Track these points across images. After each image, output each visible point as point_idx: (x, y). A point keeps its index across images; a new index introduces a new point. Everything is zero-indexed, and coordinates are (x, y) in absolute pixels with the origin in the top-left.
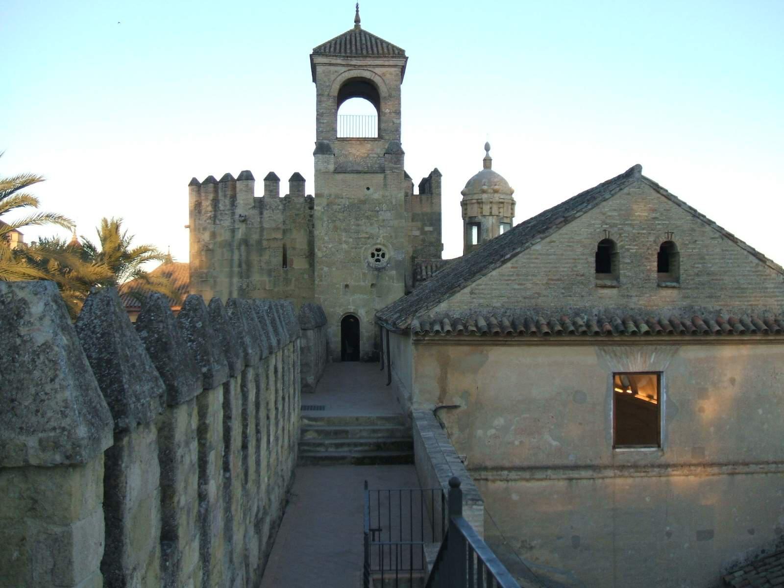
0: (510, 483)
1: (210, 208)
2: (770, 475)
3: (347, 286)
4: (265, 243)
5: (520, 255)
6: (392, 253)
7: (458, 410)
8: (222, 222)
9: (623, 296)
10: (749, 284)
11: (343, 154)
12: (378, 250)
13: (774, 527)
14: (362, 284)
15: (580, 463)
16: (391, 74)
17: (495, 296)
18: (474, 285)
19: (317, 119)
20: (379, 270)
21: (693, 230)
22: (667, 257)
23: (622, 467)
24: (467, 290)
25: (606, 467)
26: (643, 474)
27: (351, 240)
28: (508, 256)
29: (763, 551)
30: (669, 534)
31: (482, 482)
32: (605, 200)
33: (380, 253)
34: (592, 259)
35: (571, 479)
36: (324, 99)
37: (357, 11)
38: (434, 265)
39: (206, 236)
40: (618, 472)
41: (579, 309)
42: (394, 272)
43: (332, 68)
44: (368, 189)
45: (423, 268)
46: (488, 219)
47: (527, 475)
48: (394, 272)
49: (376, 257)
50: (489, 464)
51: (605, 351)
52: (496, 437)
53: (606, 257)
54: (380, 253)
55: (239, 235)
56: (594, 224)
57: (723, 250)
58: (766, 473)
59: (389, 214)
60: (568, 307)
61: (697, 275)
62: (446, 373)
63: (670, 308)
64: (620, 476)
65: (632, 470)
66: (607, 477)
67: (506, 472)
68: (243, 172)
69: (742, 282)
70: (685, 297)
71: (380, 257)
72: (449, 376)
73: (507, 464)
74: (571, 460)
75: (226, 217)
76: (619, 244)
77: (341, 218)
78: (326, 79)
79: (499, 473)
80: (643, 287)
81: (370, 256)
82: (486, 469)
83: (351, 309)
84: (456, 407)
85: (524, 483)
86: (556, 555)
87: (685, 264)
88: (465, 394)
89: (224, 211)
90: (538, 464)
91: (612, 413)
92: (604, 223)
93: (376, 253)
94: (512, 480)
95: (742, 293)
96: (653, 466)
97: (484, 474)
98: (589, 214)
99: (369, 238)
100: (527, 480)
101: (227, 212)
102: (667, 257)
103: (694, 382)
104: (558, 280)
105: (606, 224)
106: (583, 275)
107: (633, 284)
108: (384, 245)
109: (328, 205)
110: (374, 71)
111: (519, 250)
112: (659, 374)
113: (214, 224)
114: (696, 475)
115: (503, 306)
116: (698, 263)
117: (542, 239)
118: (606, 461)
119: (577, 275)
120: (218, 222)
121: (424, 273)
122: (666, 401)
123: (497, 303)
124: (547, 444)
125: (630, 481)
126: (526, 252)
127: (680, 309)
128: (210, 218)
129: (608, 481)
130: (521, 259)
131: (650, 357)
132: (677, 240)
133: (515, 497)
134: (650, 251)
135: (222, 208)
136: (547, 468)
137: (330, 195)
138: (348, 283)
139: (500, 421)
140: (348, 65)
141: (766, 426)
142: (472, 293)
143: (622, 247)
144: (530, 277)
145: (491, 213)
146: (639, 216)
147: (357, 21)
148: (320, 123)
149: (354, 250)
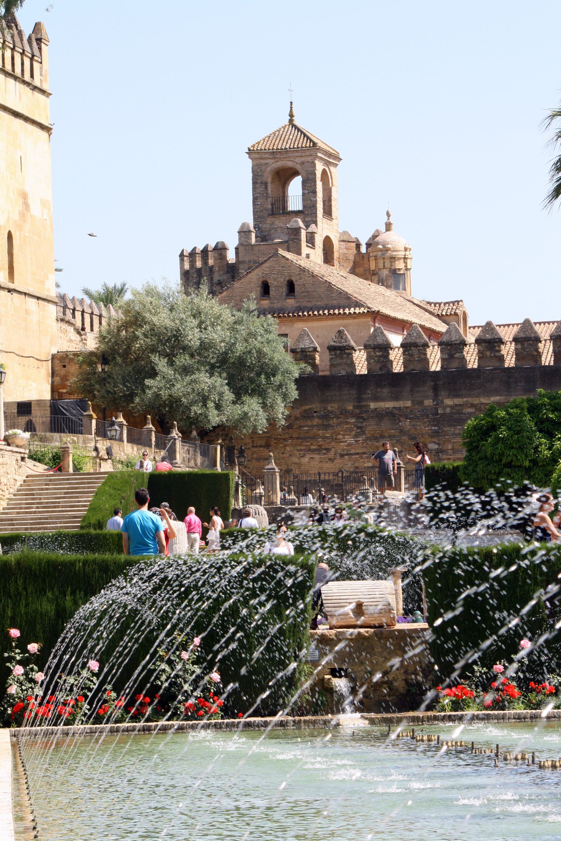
1: (195, 275)
16: (308, 162)
19: (254, 202)
22: (291, 287)
36: (257, 185)
37: (291, 108)
43: (263, 161)
68: (218, 243)
70: (298, 302)
78: (259, 170)
87: (297, 288)
102: (291, 287)
132: (294, 279)
137: (250, 261)
140: (274, 158)
145: (384, 266)
147: (291, 115)
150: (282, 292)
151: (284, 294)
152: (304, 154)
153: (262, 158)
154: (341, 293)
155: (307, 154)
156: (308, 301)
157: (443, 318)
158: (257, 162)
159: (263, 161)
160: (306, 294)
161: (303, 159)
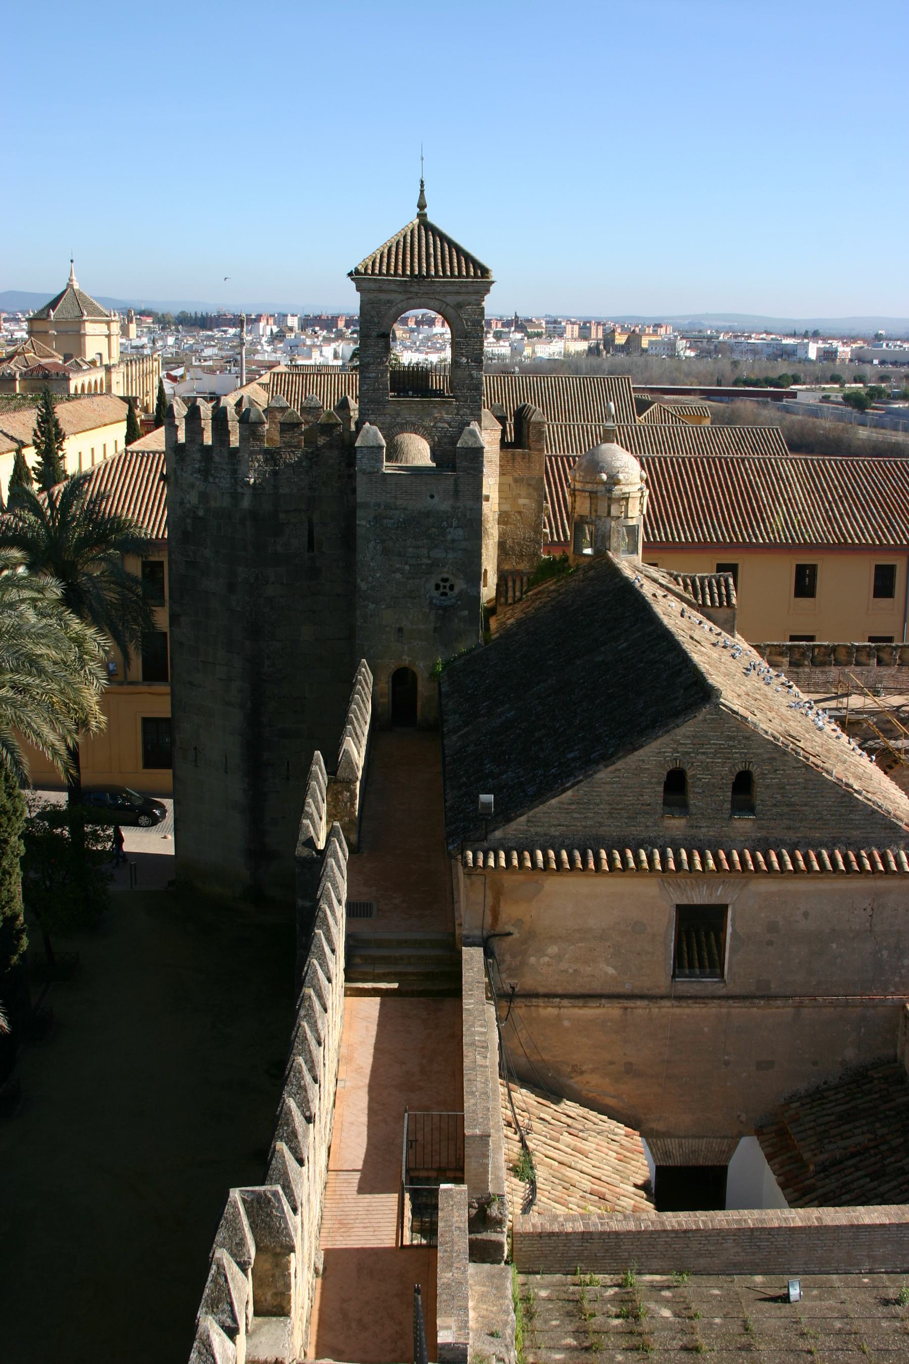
0: (562, 1010)
1: (198, 456)
2: (839, 1009)
3: (400, 630)
4: (282, 516)
5: (582, 784)
6: (464, 586)
7: (511, 938)
8: (217, 480)
9: (692, 827)
10: (832, 815)
11: (398, 423)
12: (445, 580)
13: (840, 1059)
14: (422, 627)
15: (636, 991)
17: (554, 826)
18: (531, 813)
20: (445, 609)
21: (774, 759)
22: (743, 783)
23: (679, 998)
24: (523, 819)
25: (662, 997)
26: (702, 1005)
27: (407, 567)
28: (569, 784)
29: (825, 1083)
30: (727, 1063)
31: (533, 1008)
32: (678, 726)
33: (448, 584)
34: (661, 789)
35: (626, 1008)
37: (422, 192)
38: (525, 579)
39: (193, 498)
40: (675, 1003)
41: (643, 840)
42: (466, 613)
43: (383, 296)
44: (432, 497)
45: (510, 584)
46: (605, 522)
47: (580, 1002)
48: (466, 613)
49: (442, 590)
50: (541, 990)
51: (669, 884)
52: (549, 965)
53: (676, 784)
54: (448, 584)
55: (246, 503)
56: (664, 752)
57: (806, 780)
58: (835, 1007)
59: (460, 532)
60: (632, 837)
61: (775, 805)
62: (499, 902)
63: (742, 839)
64: (677, 1007)
65: (690, 1001)
66: (663, 1007)
67: (558, 1000)
69: (825, 813)
70: (761, 828)
71: (447, 590)
72: (502, 904)
73: (560, 990)
74: (627, 988)
75: (223, 474)
76: (690, 773)
77: (394, 537)
78: (374, 313)
79: (551, 1000)
80: (714, 818)
81: (434, 587)
82: (537, 996)
83: (406, 661)
84: (510, 934)
85: (576, 1010)
86: (607, 1080)
87: (761, 794)
88: (519, 922)
89: (220, 463)
90: (591, 992)
91: (672, 945)
92: (675, 750)
93: (442, 584)
94: (563, 1007)
95: (824, 824)
96: (714, 997)
97: (535, 1001)
98: (659, 741)
99: (432, 565)
100: (580, 1007)
101: (225, 467)
102: (743, 783)
103: (763, 915)
104: (621, 809)
105: (678, 752)
106: (649, 805)
107: (703, 814)
108: (453, 574)
109: (375, 517)
110: (445, 300)
111: (581, 778)
112: (725, 907)
113: (206, 480)
114: (758, 1008)
115: (561, 835)
116: (777, 793)
117: (606, 766)
118: (663, 991)
119: (642, 804)
120: (211, 480)
121: (510, 594)
122: (731, 934)
123: (554, 832)
124: (604, 972)
125: (688, 1011)
126: (589, 780)
127: (753, 841)
128: (199, 471)
129: (664, 1010)
130: (583, 788)
131: (717, 890)
132: (755, 770)
133: (566, 1023)
134: (724, 781)
135: (217, 459)
136: (600, 996)
137: (379, 505)
138: (402, 625)
139: (553, 950)
140: (406, 292)
141: (839, 960)
142: (528, 821)
143: (694, 776)
144: (591, 807)
146: (714, 744)
147: (422, 206)
148: (365, 377)
149: (411, 581)
150: (724, 801)
151: (728, 806)
152: (464, 290)
153: (381, 291)
154: (874, 812)
155: (471, 289)
156: (789, 828)
157: (706, 610)
158: (371, 296)
159: (383, 296)
160: (786, 809)
161: (460, 298)
